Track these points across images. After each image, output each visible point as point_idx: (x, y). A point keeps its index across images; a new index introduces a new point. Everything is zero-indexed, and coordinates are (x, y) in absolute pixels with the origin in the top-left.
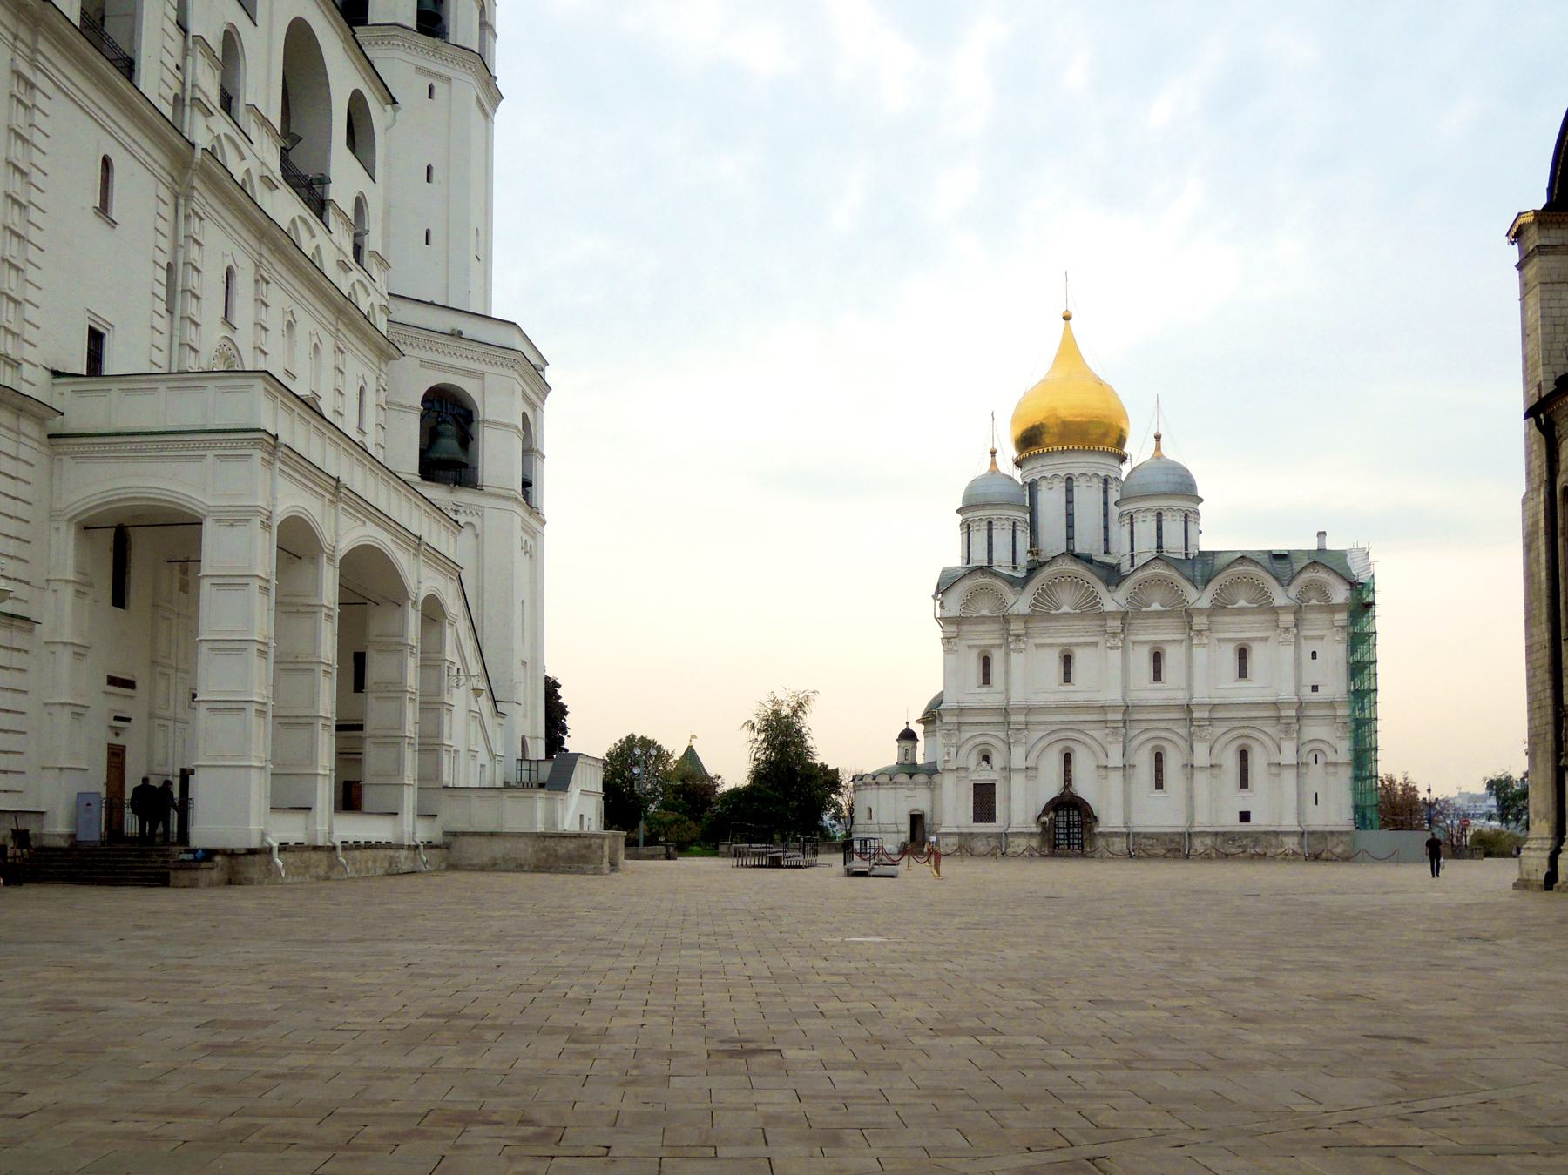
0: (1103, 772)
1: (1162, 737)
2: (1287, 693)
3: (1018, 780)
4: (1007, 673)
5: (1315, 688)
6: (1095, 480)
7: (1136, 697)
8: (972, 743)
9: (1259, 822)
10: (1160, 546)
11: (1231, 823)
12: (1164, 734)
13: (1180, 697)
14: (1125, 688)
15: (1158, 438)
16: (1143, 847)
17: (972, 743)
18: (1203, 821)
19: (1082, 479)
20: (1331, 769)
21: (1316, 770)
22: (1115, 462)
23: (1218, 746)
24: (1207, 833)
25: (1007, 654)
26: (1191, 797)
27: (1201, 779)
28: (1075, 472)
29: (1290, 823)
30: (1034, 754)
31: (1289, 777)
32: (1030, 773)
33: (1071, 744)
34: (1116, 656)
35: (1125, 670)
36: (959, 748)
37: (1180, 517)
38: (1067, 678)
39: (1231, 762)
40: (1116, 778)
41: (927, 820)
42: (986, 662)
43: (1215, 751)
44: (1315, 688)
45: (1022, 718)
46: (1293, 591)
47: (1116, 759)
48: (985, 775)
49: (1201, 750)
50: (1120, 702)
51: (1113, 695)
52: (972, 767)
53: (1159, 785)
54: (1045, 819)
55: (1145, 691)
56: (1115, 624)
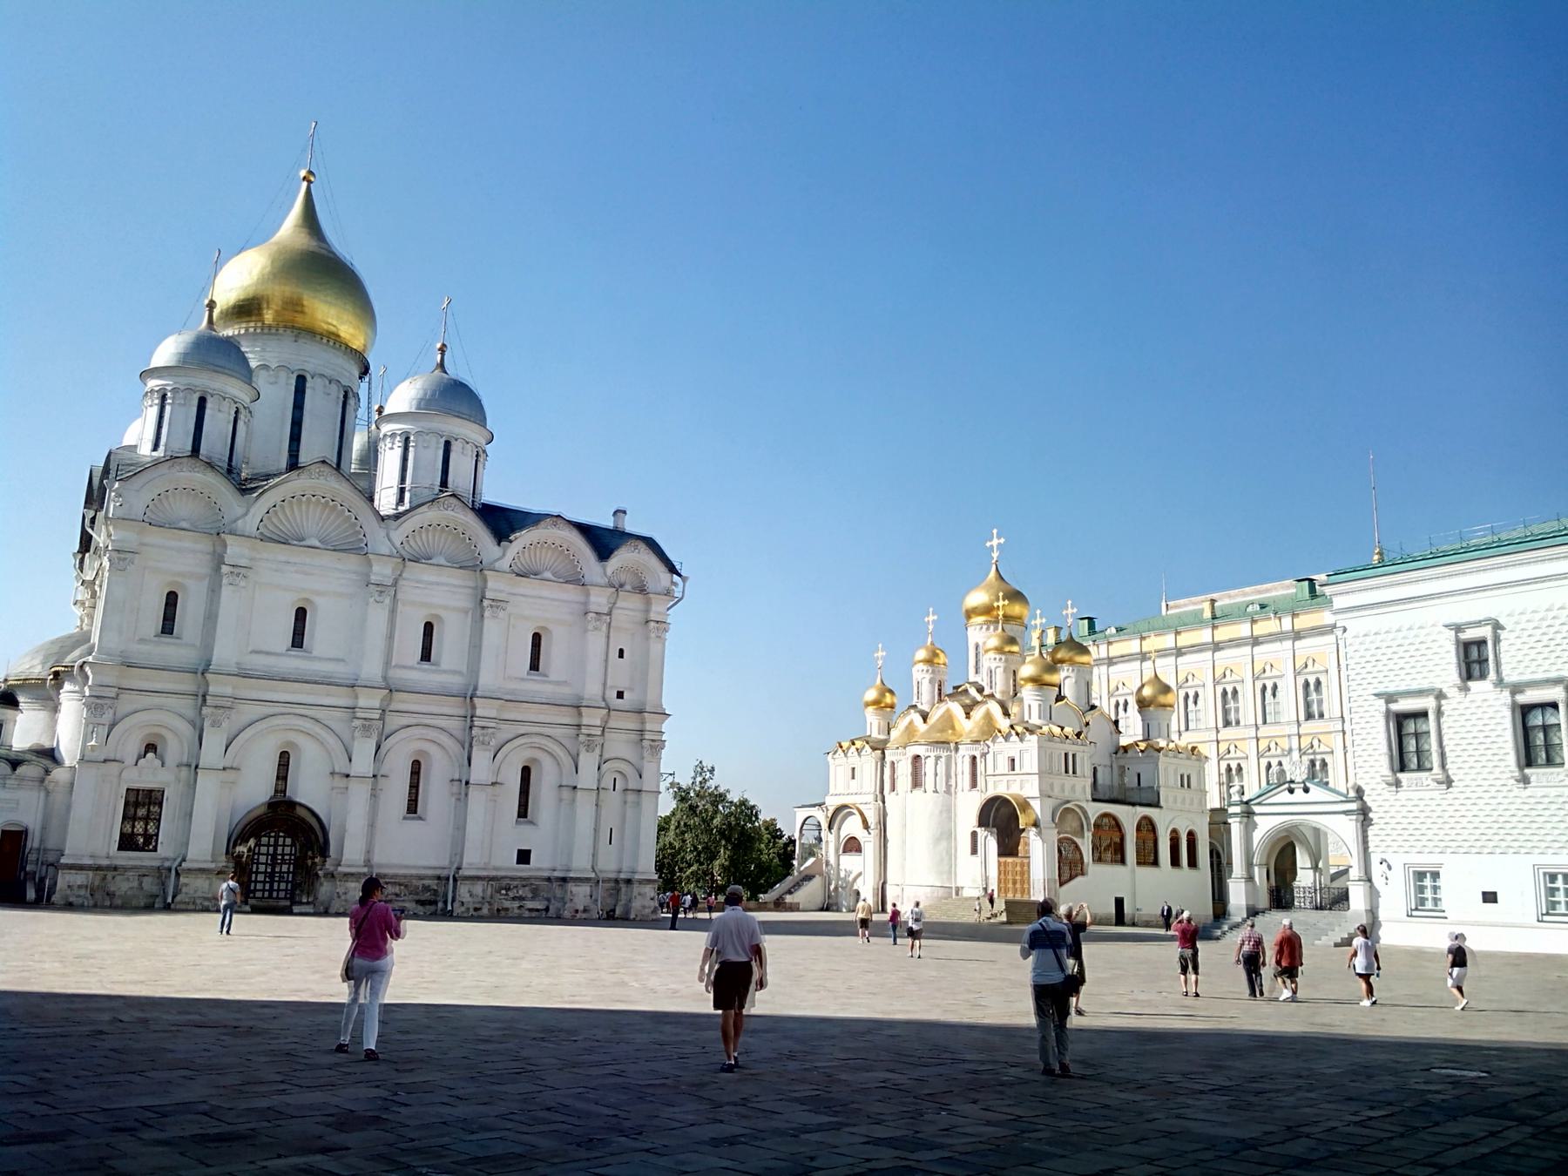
0: (341, 782)
2: (592, 690)
3: (207, 785)
4: (211, 618)
5: (620, 695)
6: (334, 387)
7: (396, 674)
10: (444, 483)
12: (433, 734)
13: (456, 682)
14: (387, 663)
15: (442, 350)
18: (473, 860)
19: (318, 380)
20: (631, 797)
22: (357, 374)
24: (479, 878)
25: (214, 591)
26: (460, 827)
27: (476, 798)
28: (308, 367)
29: (581, 864)
32: (230, 775)
33: (292, 737)
34: (378, 616)
36: (112, 726)
37: (470, 452)
38: (298, 640)
40: (359, 794)
41: (33, 842)
42: (172, 600)
44: (620, 695)
45: (228, 691)
47: (363, 763)
48: (148, 776)
49: (481, 757)
50: (379, 681)
51: (372, 669)
52: (130, 760)
53: (412, 806)
54: (242, 849)
56: (382, 571)
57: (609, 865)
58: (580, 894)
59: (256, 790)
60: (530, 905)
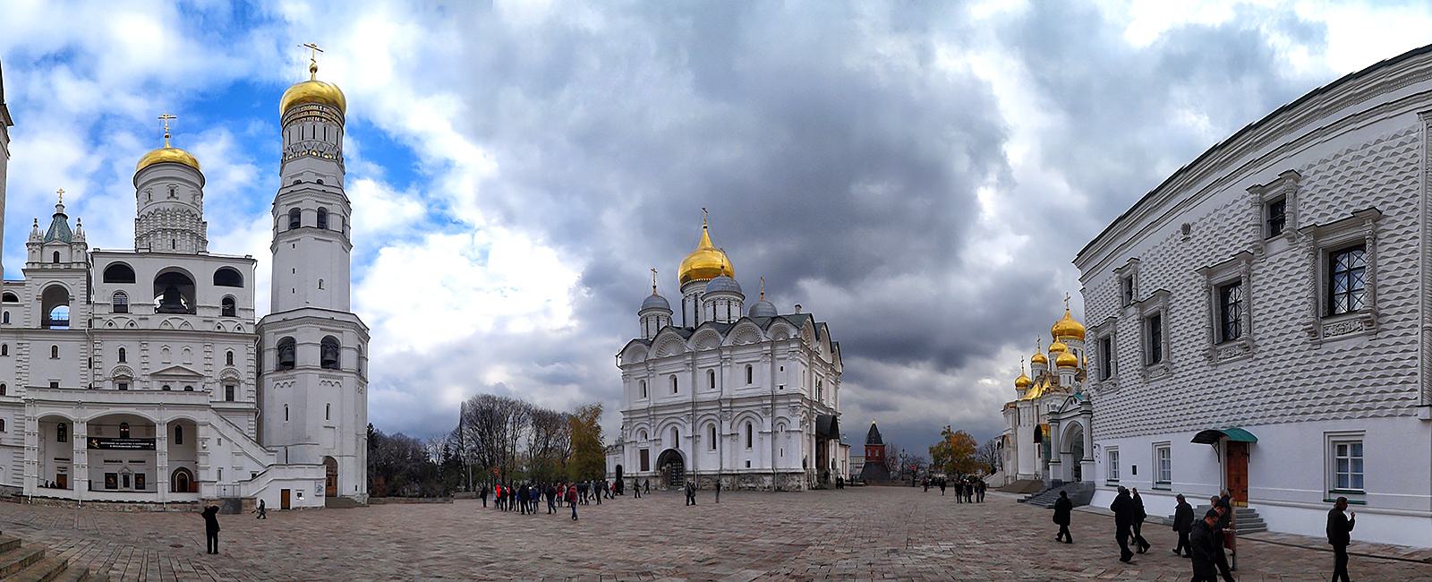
1: (714, 416)
5: (781, 387)
8: (636, 429)
9: (755, 466)
10: (715, 318)
11: (742, 467)
14: (694, 393)
16: (716, 484)
17: (636, 429)
21: (781, 435)
23: (737, 422)
29: (768, 467)
30: (659, 431)
31: (768, 440)
35: (694, 382)
39: (743, 431)
43: (734, 426)
46: (770, 335)
49: (726, 425)
55: (706, 394)
57: (782, 466)
58: (768, 481)
59: (667, 444)
60: (750, 485)
